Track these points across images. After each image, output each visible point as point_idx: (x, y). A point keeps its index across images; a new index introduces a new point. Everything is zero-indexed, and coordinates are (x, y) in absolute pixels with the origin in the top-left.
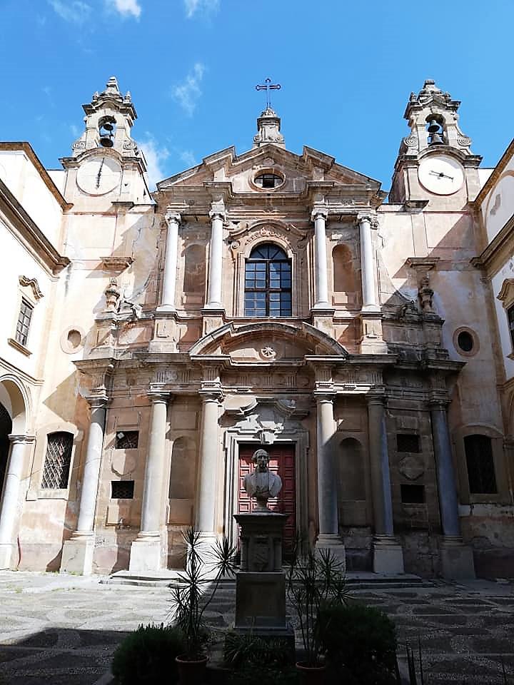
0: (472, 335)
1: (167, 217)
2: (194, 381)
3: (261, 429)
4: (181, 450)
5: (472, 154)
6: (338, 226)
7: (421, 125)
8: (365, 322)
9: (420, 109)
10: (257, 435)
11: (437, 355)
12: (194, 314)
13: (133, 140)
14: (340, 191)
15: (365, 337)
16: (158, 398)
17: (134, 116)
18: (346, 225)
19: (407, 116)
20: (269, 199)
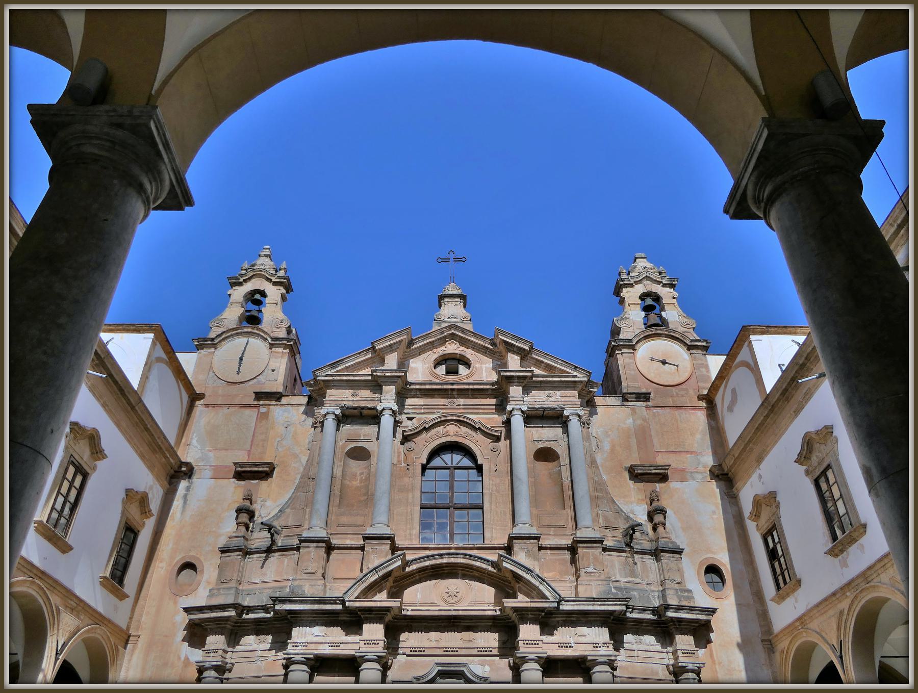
7: (634, 304)
9: (631, 285)
12: (352, 539)
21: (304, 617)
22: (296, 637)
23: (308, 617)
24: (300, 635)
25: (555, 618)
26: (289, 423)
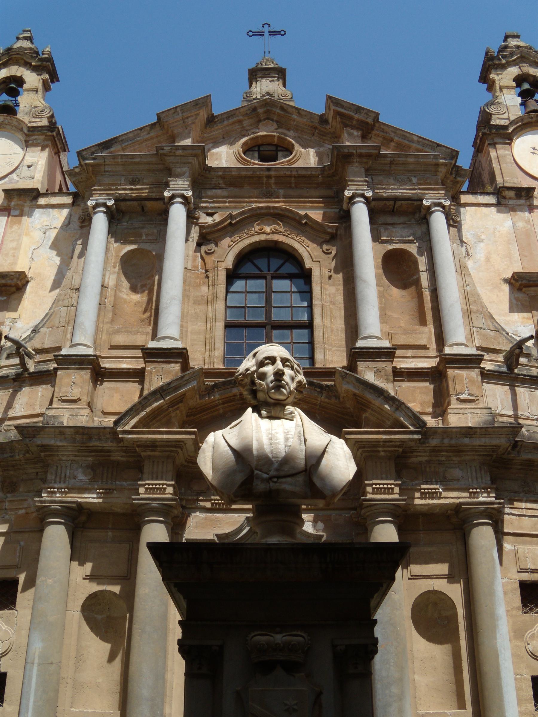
1: (90, 203)
2: (125, 483)
4: (99, 617)
6: (389, 219)
7: (508, 87)
8: (450, 372)
9: (504, 67)
13: (48, 105)
14: (391, 163)
15: (453, 399)
16: (55, 514)
17: (54, 77)
18: (402, 219)
19: (484, 78)
20: (269, 177)
21: (63, 455)
22: (53, 482)
23: (68, 456)
24: (58, 479)
25: (416, 457)
26: (48, 227)
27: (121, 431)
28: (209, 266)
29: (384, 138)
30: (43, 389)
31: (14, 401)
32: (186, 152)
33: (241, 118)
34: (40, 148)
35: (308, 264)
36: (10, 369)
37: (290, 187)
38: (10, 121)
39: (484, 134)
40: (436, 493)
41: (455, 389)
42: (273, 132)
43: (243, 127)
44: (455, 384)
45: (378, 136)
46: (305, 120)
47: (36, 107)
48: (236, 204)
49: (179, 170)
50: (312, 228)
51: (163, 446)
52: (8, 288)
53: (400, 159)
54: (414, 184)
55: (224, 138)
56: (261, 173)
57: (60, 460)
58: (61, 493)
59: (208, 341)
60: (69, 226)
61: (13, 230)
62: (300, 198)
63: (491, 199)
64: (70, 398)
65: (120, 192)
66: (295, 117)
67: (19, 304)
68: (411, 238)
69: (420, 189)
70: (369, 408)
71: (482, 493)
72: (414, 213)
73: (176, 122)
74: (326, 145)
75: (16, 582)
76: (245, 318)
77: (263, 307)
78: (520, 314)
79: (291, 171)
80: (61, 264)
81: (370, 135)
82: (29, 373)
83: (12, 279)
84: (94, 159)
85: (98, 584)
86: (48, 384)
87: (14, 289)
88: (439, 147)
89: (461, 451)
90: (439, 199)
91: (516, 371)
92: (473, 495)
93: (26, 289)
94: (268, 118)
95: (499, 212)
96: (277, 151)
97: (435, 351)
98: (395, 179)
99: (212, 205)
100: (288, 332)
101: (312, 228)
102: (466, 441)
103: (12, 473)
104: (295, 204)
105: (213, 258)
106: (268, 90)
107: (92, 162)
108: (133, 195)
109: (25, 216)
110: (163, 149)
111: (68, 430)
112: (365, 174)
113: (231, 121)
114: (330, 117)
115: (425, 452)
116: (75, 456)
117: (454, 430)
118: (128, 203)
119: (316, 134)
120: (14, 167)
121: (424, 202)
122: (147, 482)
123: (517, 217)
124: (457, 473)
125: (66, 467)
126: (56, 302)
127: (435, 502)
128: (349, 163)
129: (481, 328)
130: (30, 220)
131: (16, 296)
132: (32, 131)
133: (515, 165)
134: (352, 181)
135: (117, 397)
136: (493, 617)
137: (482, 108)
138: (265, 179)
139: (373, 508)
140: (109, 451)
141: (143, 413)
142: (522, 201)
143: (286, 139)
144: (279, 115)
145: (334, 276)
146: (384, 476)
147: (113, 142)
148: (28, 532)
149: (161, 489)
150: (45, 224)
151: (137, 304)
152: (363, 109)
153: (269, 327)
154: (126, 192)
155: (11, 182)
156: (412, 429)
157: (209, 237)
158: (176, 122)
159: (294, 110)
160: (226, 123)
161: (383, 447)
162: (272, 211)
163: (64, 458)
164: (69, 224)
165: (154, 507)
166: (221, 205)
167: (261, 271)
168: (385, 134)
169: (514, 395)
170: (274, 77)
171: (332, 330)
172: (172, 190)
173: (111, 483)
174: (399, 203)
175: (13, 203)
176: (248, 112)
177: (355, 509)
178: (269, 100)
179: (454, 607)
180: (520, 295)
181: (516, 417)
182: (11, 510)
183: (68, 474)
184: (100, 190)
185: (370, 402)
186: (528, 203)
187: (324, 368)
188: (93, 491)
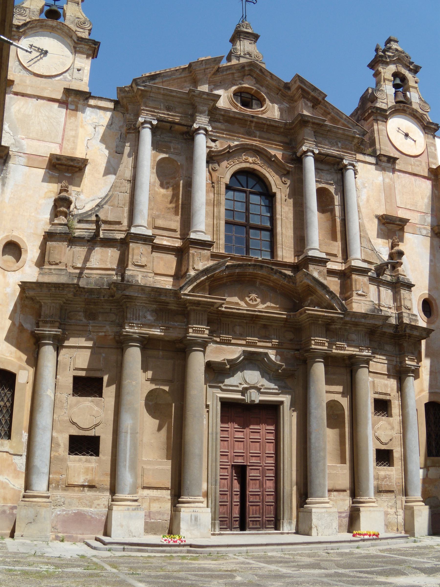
0: (433, 302)
2: (176, 324)
3: (246, 386)
5: (431, 121)
7: (388, 80)
8: (354, 277)
9: (387, 64)
10: (244, 392)
11: (410, 319)
12: (168, 241)
13: (88, 19)
14: (328, 131)
20: (252, 122)
21: (138, 302)
22: (131, 319)
23: (141, 303)
24: (134, 317)
25: (335, 325)
26: (97, 124)
27: (183, 294)
28: (215, 179)
29: (325, 111)
30: (112, 251)
31: (90, 256)
32: (209, 97)
33: (234, 71)
34: (86, 56)
35: (274, 189)
36: (83, 232)
37: (263, 131)
38: (62, 27)
39: (372, 112)
40: (343, 347)
41: (356, 287)
42: (252, 86)
43: (234, 78)
44: (356, 284)
45: (322, 108)
46: (275, 83)
47: (79, 18)
48: (230, 137)
49: (201, 108)
50: (276, 164)
51: (203, 305)
52: (74, 168)
53: (334, 130)
54: (338, 148)
55: (220, 83)
56: (248, 118)
57: (136, 305)
58: (138, 327)
59: (215, 232)
60: (112, 126)
61: (71, 121)
62: (268, 140)
63: (372, 160)
64: (140, 264)
65: (161, 115)
66: (269, 79)
67: (81, 181)
68: (332, 182)
69: (342, 152)
70: (315, 294)
71: (365, 350)
72: (334, 164)
73: (200, 70)
74: (284, 103)
75: (101, 380)
76: (234, 219)
77: (244, 212)
78: (382, 240)
79: (266, 121)
80: (109, 155)
81: (316, 107)
82: (101, 238)
83: (78, 163)
84: (144, 86)
85: (156, 385)
86: (115, 248)
87: (77, 169)
88: (357, 126)
89: (357, 325)
90: (352, 161)
91: (381, 277)
92: (361, 350)
93: (85, 171)
94: (249, 75)
95: (376, 169)
96: (252, 99)
97: (341, 259)
98: (330, 142)
99: (215, 134)
100: (258, 232)
101: (276, 164)
102: (363, 320)
103: (92, 307)
104: (266, 144)
105: (217, 174)
106: (248, 50)
107: (143, 88)
108: (169, 119)
109: (79, 111)
110: (194, 92)
111: (147, 288)
112: (314, 135)
113: (228, 72)
114: (294, 88)
115: (340, 323)
116: (146, 303)
117: (358, 314)
118: (164, 123)
119: (279, 94)
120: (67, 68)
121: (344, 161)
122: (194, 326)
123: (385, 175)
124: (354, 337)
125: (139, 310)
126: (113, 187)
127: (342, 352)
128: (306, 126)
129: (365, 248)
130: (84, 115)
131: (78, 174)
132: (80, 41)
133: (387, 138)
134: (307, 140)
135: (162, 263)
136: (366, 417)
137: (370, 91)
138: (249, 122)
139: (314, 353)
140: (168, 303)
141: (195, 283)
142: (389, 165)
143: (261, 94)
144: (257, 74)
145: (288, 200)
146: (320, 335)
147: (158, 76)
148: (108, 348)
149: (202, 331)
150: (95, 121)
151: (164, 195)
152: (318, 90)
153: (248, 227)
154: (165, 116)
155: (65, 78)
156: (339, 311)
157: (214, 158)
158: (200, 70)
159: (269, 74)
160: (225, 73)
161: (322, 319)
162: (254, 148)
163: (138, 304)
164: (112, 124)
165: (199, 342)
166: (221, 135)
167: (243, 187)
168: (326, 109)
169: (379, 291)
170: (252, 40)
171: (286, 236)
172: (199, 124)
173: (168, 323)
174: (328, 158)
175: (70, 99)
176: (240, 68)
177: (298, 350)
178: (253, 62)
179: (343, 409)
180: (383, 227)
181: (379, 305)
182: (94, 332)
183: (141, 315)
184: (147, 110)
185: (317, 291)
186: (393, 167)
187: (282, 261)
188: (157, 327)
